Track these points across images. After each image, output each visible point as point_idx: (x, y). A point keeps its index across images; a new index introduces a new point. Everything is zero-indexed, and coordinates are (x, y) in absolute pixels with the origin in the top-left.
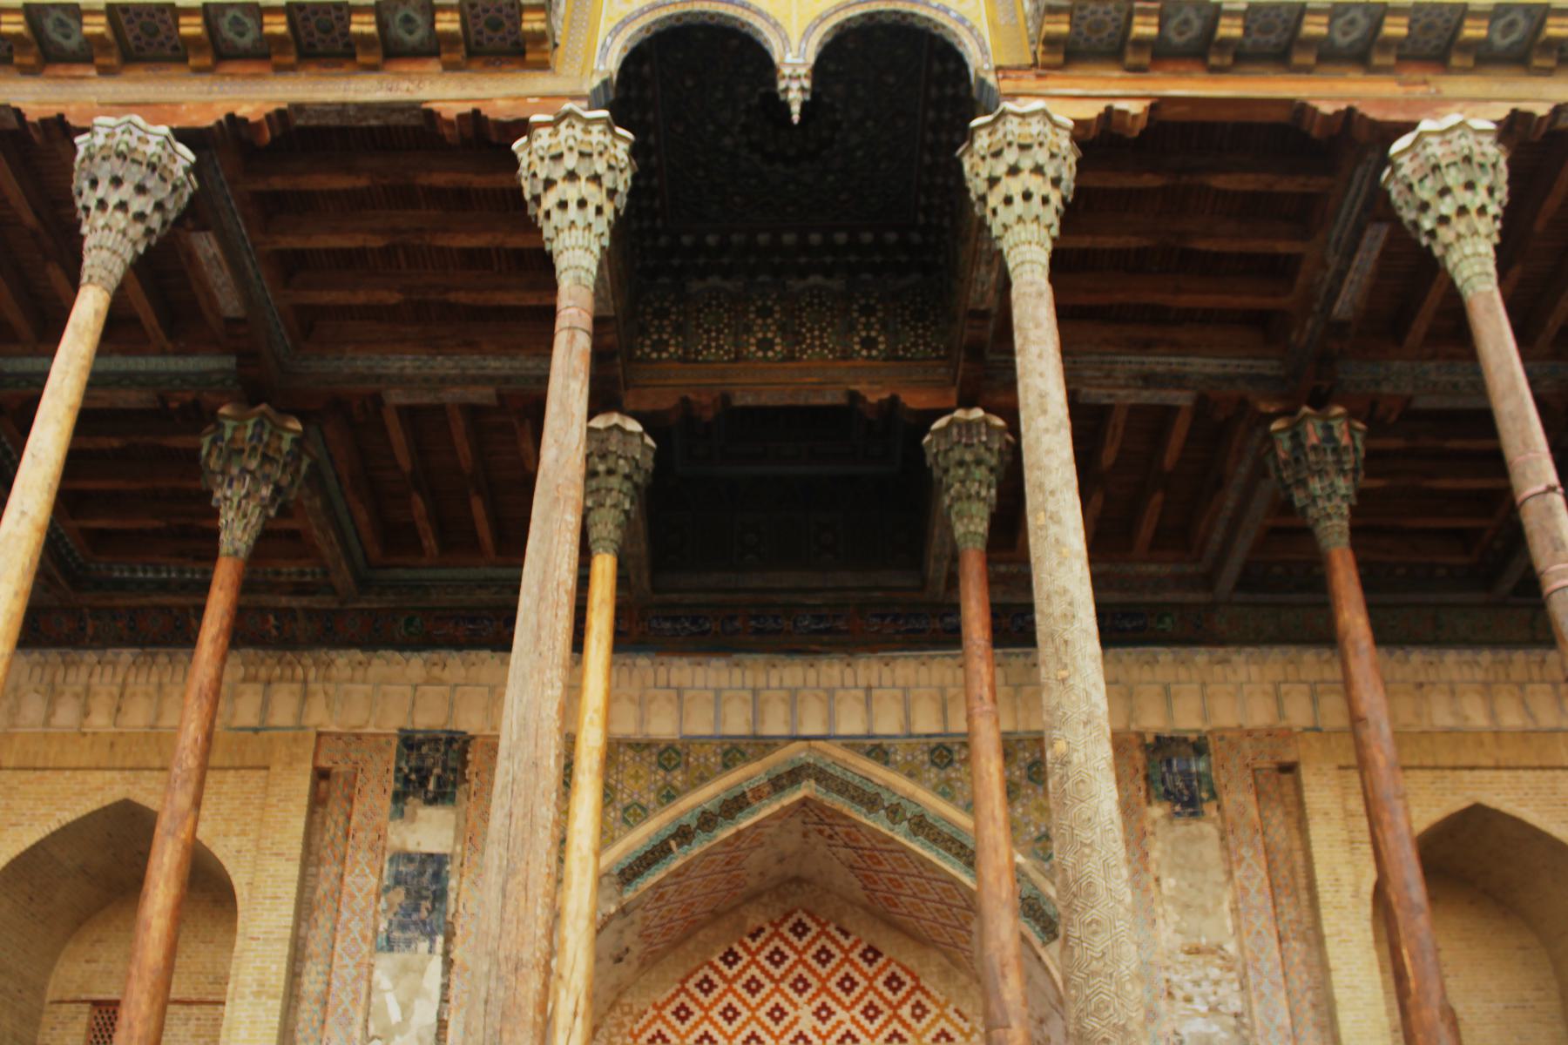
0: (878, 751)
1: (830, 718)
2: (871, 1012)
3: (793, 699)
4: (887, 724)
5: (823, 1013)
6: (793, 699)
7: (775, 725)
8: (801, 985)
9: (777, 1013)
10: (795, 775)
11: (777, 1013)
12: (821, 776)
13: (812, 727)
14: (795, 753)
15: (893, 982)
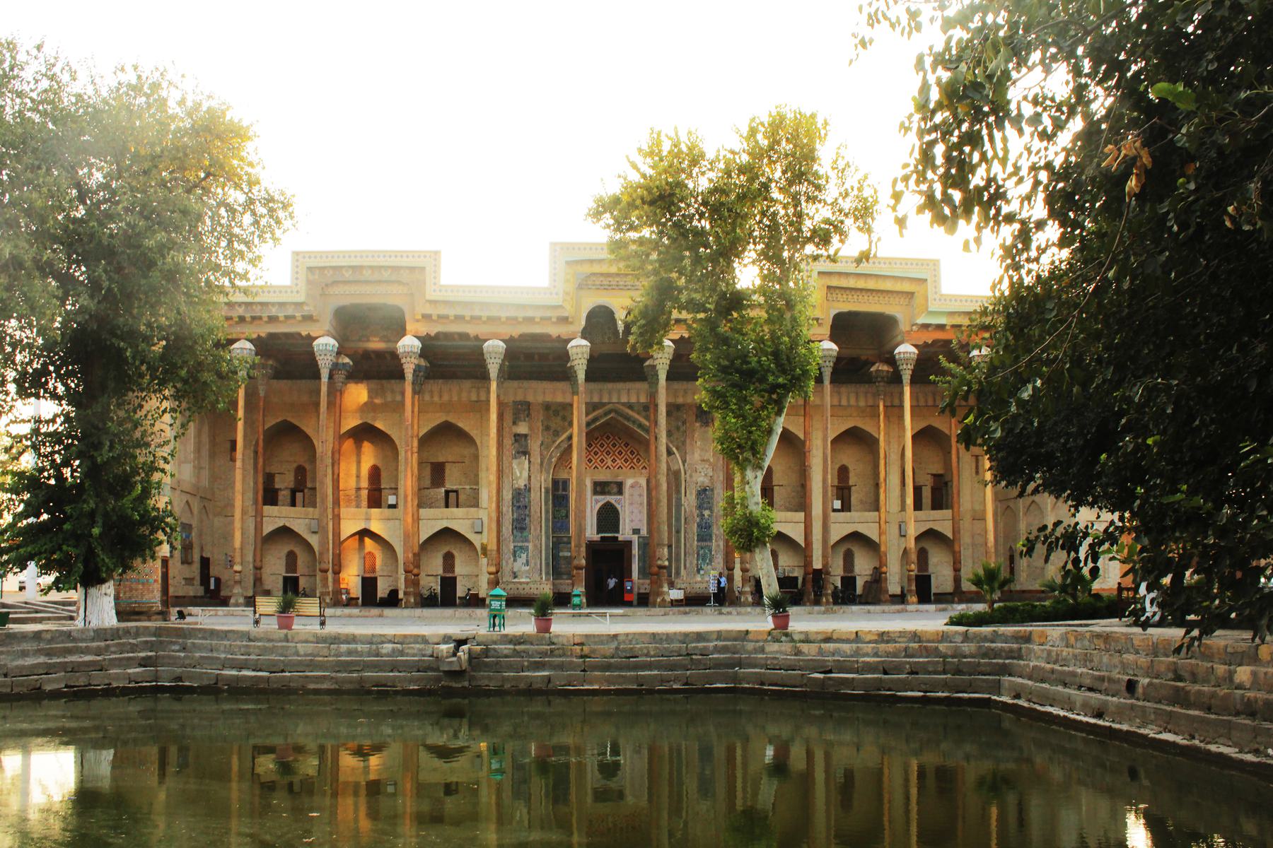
0: (630, 406)
1: (619, 397)
2: (626, 461)
3: (610, 394)
4: (633, 400)
5: (614, 461)
6: (610, 394)
7: (605, 400)
8: (608, 453)
9: (602, 461)
10: (610, 412)
11: (602, 461)
12: (616, 411)
13: (615, 400)
14: (610, 406)
15: (632, 453)
